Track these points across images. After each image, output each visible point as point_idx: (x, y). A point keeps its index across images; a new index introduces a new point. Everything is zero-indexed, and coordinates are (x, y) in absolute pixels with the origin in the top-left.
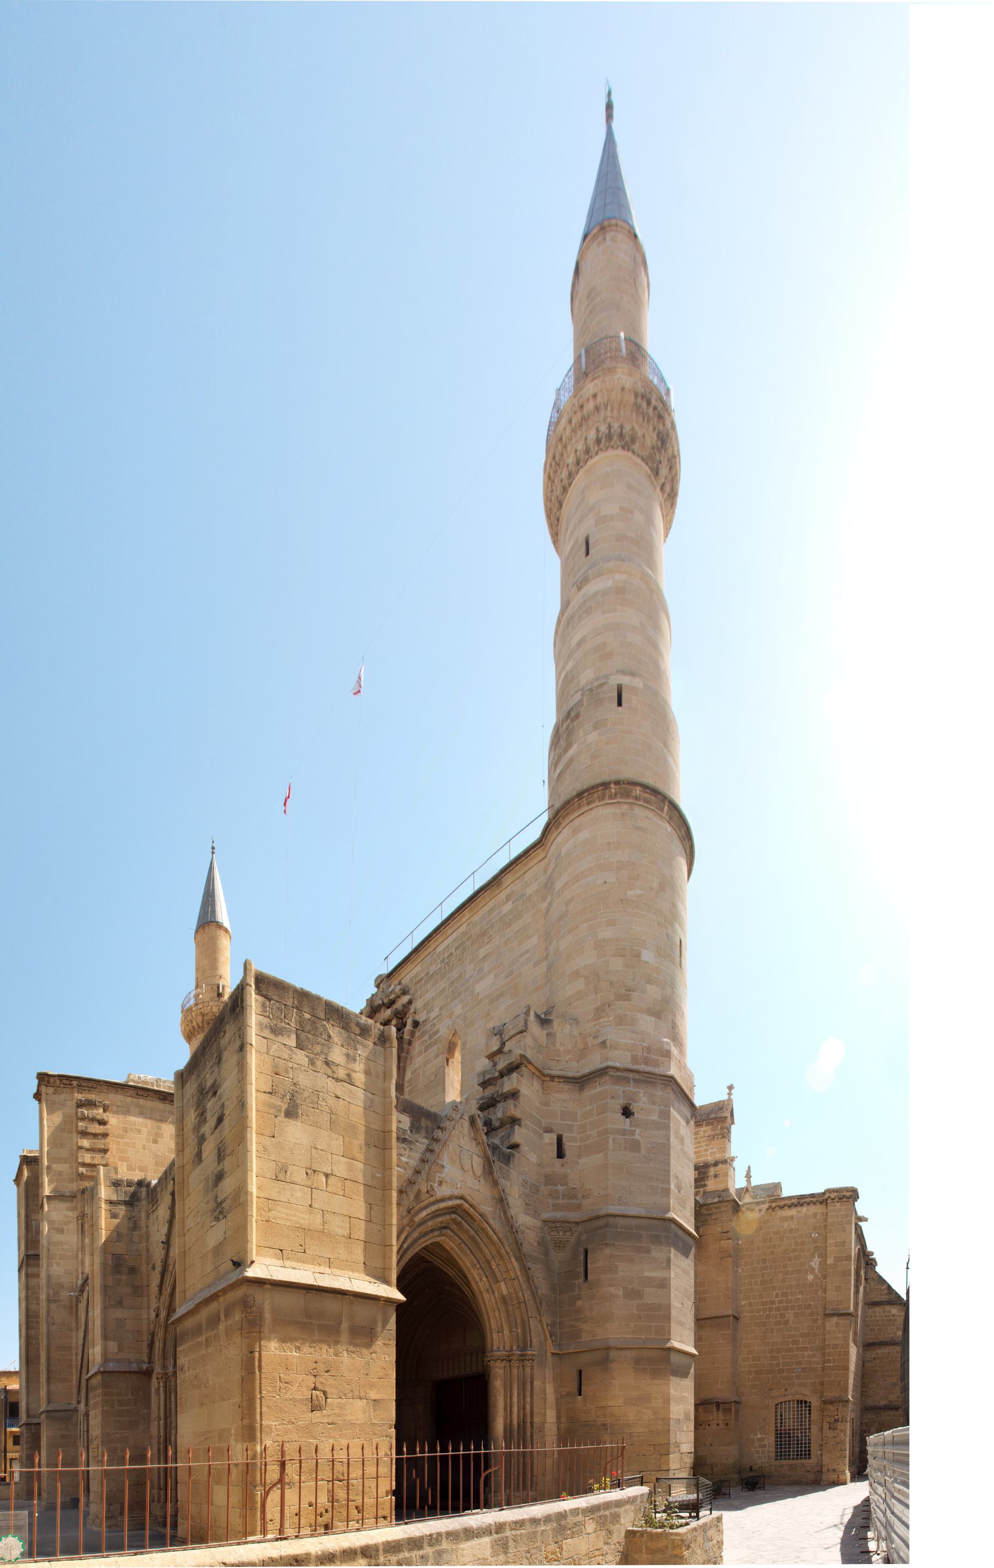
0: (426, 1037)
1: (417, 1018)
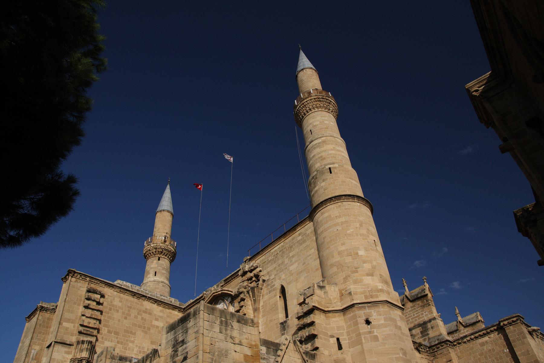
0: (269, 287)
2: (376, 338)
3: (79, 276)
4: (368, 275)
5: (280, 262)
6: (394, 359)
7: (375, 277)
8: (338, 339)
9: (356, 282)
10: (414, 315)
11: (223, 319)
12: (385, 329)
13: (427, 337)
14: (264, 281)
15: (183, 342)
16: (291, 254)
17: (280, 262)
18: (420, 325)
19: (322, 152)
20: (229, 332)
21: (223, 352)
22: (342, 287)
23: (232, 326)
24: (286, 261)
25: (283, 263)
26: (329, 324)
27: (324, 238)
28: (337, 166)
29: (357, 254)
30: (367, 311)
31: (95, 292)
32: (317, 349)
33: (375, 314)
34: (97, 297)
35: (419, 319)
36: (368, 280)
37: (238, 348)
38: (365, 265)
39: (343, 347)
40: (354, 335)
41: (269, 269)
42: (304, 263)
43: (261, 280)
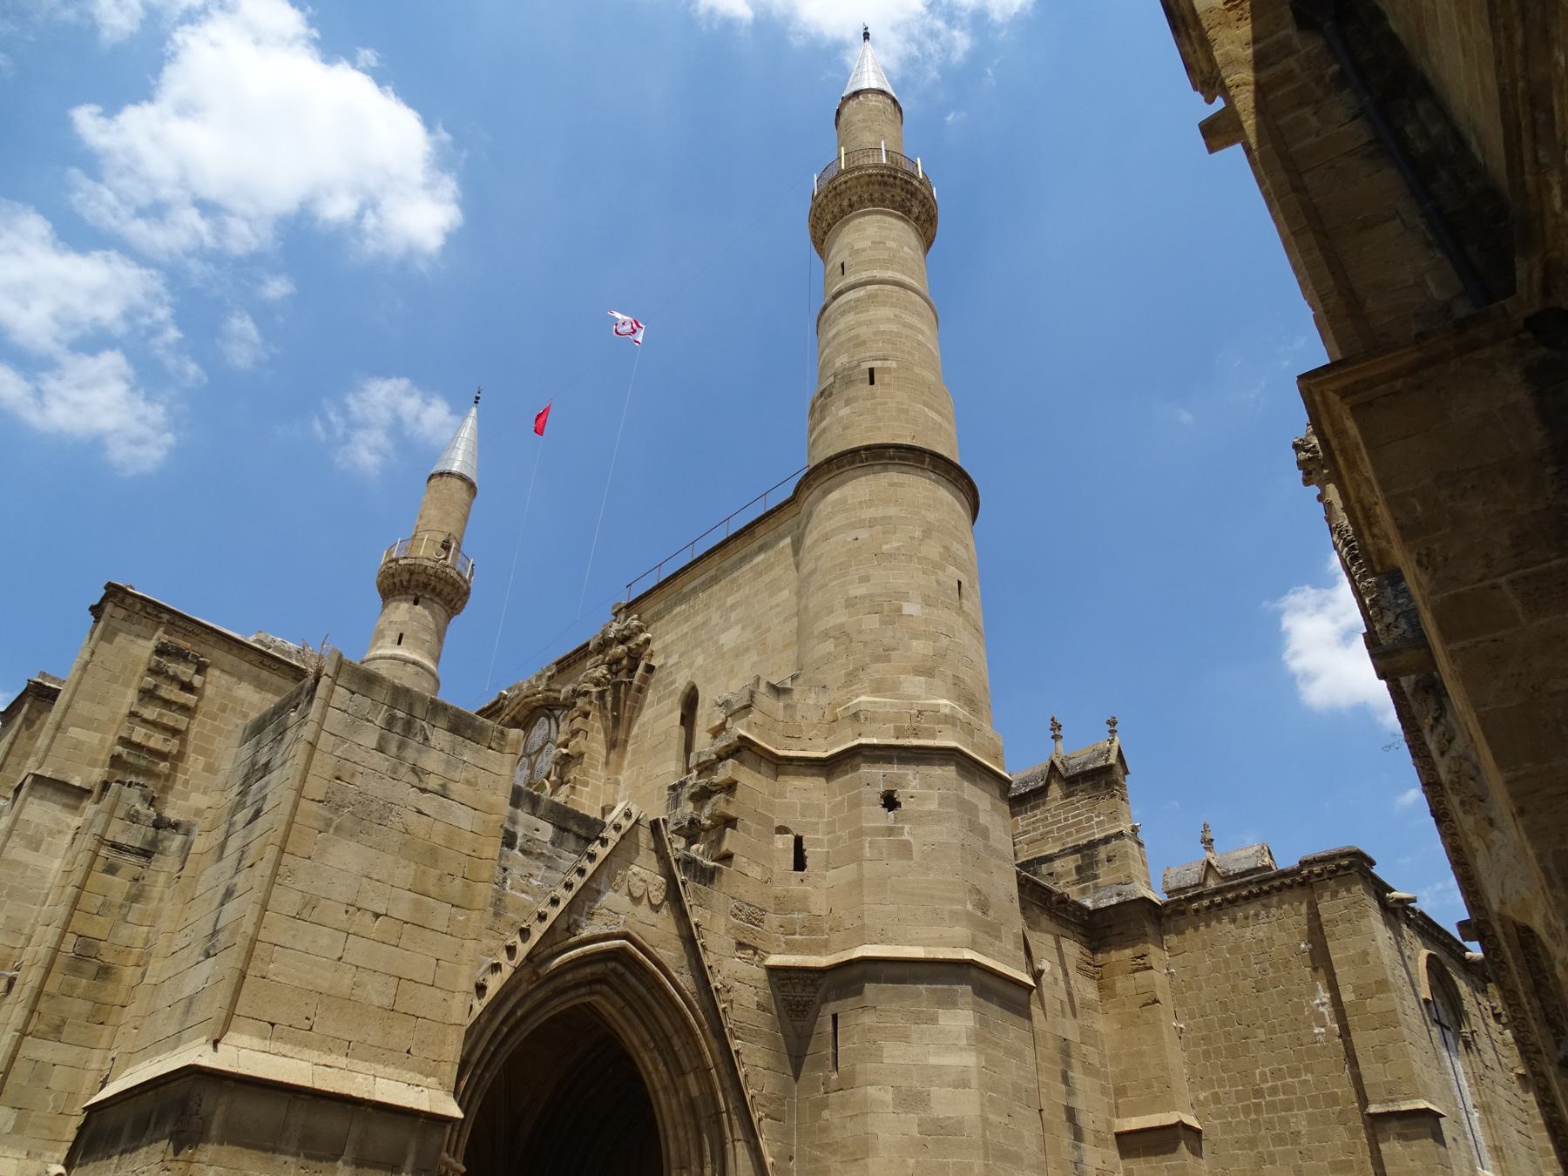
1: (653, 663)
2: (905, 850)
3: (139, 606)
4: (918, 671)
5: (699, 619)
6: (946, 916)
7: (937, 681)
8: (798, 841)
9: (878, 688)
10: (1066, 819)
11: (400, 714)
12: (936, 828)
13: (1090, 884)
14: (650, 669)
15: (267, 768)
16: (730, 601)
17: (699, 619)
18: (1077, 849)
19: (859, 324)
20: (410, 754)
21: (374, 807)
22: (836, 695)
23: (426, 739)
24: (716, 618)
25: (704, 624)
26: (783, 795)
27: (818, 559)
28: (894, 365)
29: (899, 609)
30: (894, 769)
31: (180, 655)
32: (727, 858)
33: (911, 780)
34: (185, 671)
35: (1078, 831)
36: (914, 685)
37: (429, 803)
38: (914, 643)
39: (808, 862)
40: (844, 834)
41: (668, 638)
42: (759, 627)
43: (642, 664)
